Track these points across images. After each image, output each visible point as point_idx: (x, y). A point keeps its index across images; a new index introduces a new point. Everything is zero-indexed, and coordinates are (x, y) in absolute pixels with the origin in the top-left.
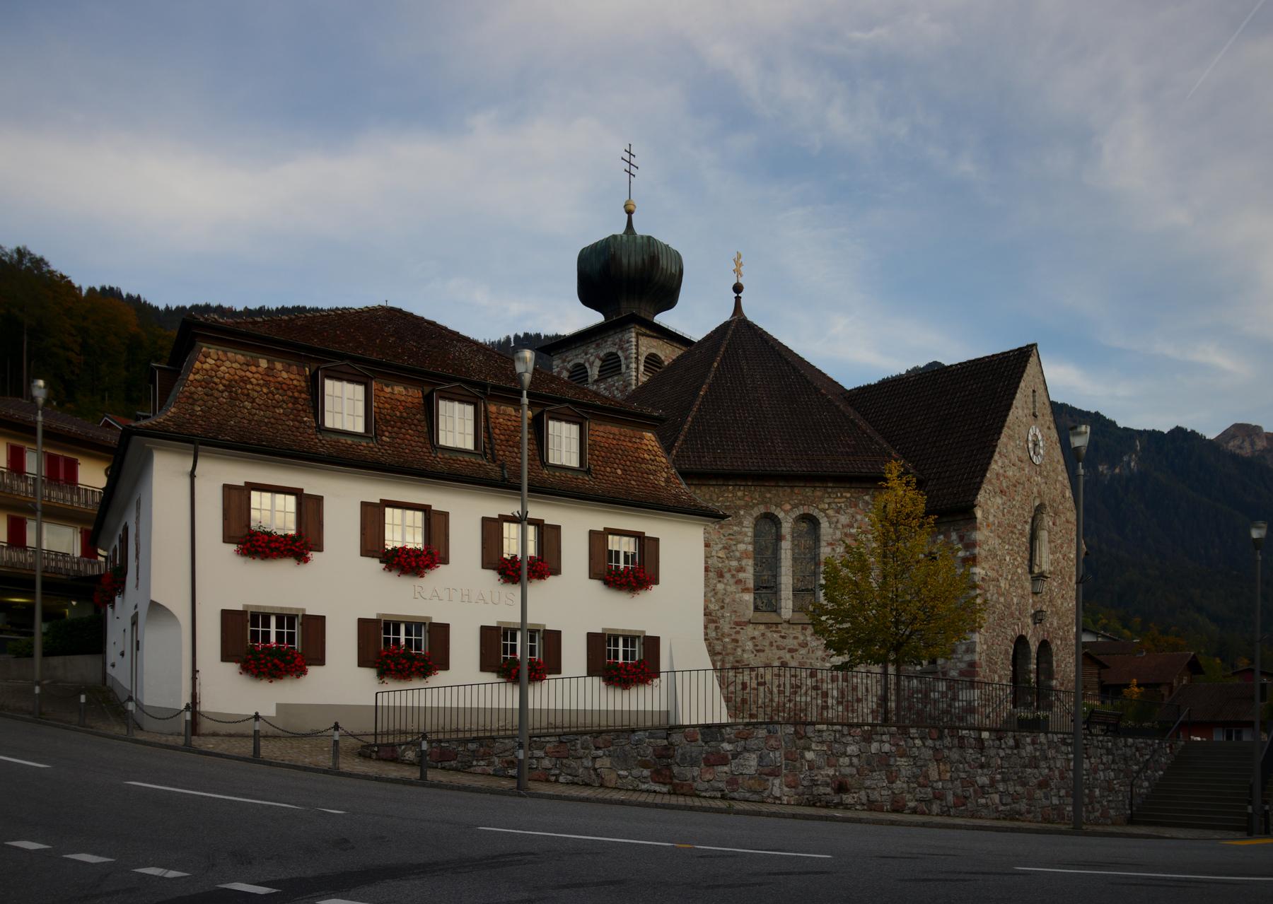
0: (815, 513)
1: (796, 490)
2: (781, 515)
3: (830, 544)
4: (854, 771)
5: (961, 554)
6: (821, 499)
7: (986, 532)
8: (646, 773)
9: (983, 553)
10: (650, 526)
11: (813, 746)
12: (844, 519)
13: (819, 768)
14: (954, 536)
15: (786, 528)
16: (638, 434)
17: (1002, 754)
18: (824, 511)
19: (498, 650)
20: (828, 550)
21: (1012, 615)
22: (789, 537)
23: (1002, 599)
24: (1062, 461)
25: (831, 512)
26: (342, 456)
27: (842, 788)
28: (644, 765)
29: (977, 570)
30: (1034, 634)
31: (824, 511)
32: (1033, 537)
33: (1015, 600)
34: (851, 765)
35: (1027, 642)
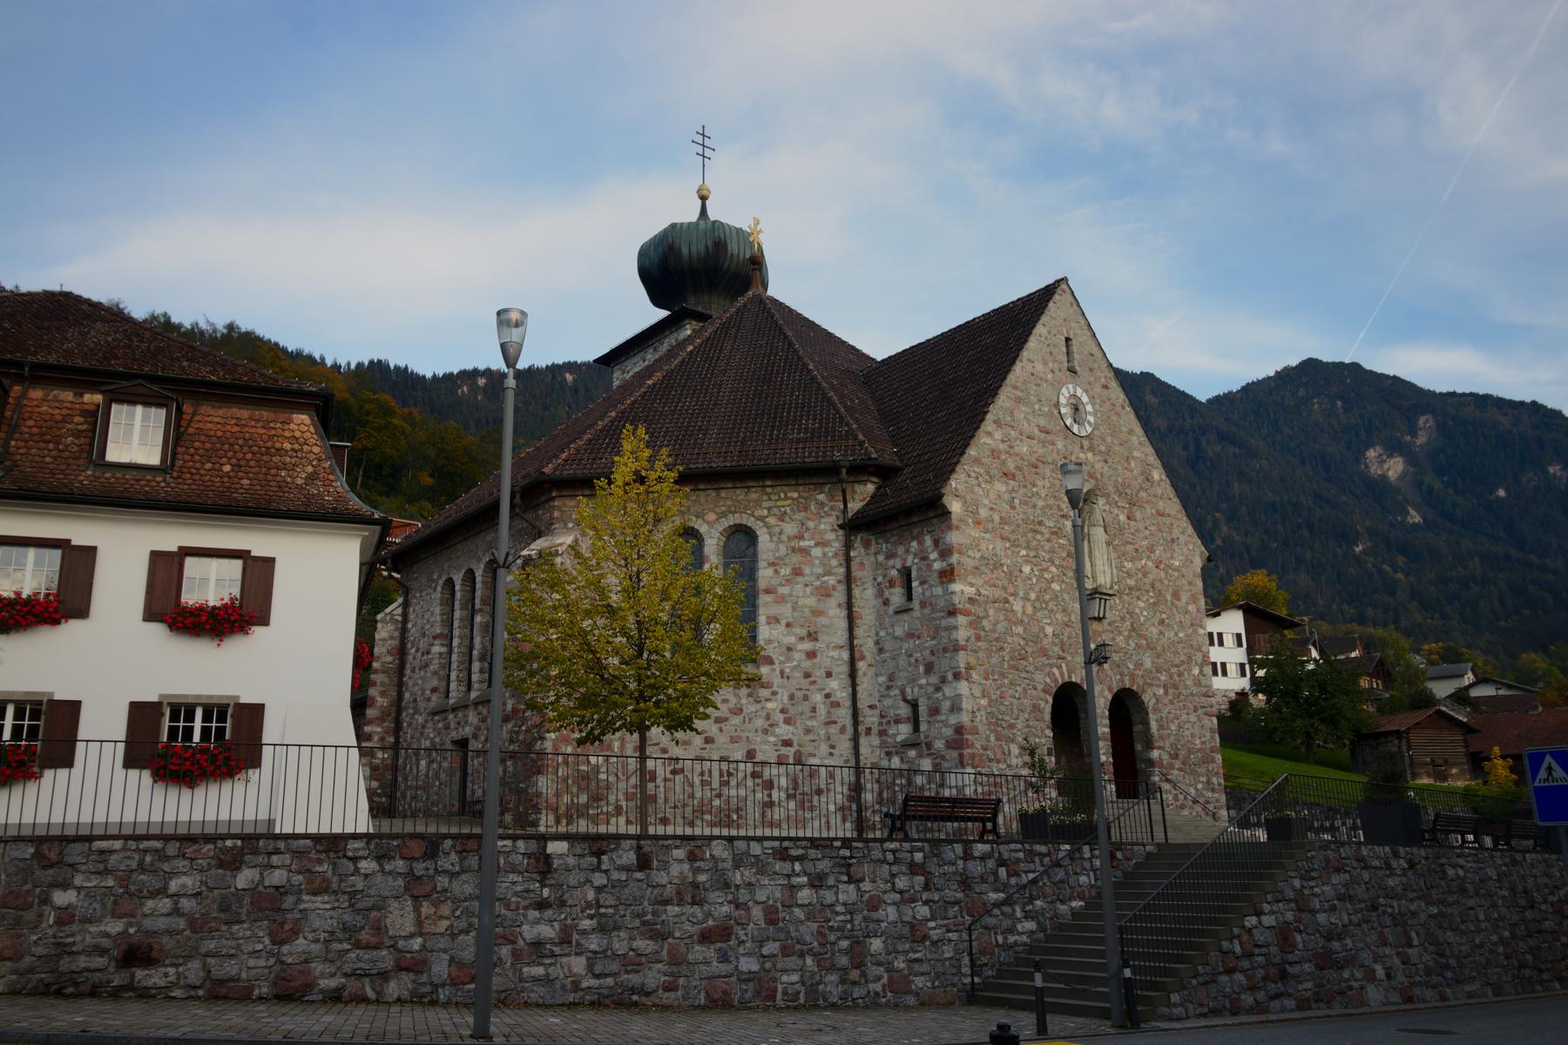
0: (751, 522)
1: (723, 494)
2: (703, 528)
4: (182, 923)
5: (937, 566)
6: (758, 503)
7: (975, 533)
9: (969, 563)
10: (259, 541)
11: (78, 880)
12: (790, 528)
13: (87, 920)
14: (928, 541)
16: (282, 417)
18: (762, 519)
20: (769, 572)
21: (1044, 652)
23: (1020, 630)
25: (772, 520)
26: (128, 495)
29: (956, 587)
31: (762, 519)
33: (1049, 630)
34: (176, 911)
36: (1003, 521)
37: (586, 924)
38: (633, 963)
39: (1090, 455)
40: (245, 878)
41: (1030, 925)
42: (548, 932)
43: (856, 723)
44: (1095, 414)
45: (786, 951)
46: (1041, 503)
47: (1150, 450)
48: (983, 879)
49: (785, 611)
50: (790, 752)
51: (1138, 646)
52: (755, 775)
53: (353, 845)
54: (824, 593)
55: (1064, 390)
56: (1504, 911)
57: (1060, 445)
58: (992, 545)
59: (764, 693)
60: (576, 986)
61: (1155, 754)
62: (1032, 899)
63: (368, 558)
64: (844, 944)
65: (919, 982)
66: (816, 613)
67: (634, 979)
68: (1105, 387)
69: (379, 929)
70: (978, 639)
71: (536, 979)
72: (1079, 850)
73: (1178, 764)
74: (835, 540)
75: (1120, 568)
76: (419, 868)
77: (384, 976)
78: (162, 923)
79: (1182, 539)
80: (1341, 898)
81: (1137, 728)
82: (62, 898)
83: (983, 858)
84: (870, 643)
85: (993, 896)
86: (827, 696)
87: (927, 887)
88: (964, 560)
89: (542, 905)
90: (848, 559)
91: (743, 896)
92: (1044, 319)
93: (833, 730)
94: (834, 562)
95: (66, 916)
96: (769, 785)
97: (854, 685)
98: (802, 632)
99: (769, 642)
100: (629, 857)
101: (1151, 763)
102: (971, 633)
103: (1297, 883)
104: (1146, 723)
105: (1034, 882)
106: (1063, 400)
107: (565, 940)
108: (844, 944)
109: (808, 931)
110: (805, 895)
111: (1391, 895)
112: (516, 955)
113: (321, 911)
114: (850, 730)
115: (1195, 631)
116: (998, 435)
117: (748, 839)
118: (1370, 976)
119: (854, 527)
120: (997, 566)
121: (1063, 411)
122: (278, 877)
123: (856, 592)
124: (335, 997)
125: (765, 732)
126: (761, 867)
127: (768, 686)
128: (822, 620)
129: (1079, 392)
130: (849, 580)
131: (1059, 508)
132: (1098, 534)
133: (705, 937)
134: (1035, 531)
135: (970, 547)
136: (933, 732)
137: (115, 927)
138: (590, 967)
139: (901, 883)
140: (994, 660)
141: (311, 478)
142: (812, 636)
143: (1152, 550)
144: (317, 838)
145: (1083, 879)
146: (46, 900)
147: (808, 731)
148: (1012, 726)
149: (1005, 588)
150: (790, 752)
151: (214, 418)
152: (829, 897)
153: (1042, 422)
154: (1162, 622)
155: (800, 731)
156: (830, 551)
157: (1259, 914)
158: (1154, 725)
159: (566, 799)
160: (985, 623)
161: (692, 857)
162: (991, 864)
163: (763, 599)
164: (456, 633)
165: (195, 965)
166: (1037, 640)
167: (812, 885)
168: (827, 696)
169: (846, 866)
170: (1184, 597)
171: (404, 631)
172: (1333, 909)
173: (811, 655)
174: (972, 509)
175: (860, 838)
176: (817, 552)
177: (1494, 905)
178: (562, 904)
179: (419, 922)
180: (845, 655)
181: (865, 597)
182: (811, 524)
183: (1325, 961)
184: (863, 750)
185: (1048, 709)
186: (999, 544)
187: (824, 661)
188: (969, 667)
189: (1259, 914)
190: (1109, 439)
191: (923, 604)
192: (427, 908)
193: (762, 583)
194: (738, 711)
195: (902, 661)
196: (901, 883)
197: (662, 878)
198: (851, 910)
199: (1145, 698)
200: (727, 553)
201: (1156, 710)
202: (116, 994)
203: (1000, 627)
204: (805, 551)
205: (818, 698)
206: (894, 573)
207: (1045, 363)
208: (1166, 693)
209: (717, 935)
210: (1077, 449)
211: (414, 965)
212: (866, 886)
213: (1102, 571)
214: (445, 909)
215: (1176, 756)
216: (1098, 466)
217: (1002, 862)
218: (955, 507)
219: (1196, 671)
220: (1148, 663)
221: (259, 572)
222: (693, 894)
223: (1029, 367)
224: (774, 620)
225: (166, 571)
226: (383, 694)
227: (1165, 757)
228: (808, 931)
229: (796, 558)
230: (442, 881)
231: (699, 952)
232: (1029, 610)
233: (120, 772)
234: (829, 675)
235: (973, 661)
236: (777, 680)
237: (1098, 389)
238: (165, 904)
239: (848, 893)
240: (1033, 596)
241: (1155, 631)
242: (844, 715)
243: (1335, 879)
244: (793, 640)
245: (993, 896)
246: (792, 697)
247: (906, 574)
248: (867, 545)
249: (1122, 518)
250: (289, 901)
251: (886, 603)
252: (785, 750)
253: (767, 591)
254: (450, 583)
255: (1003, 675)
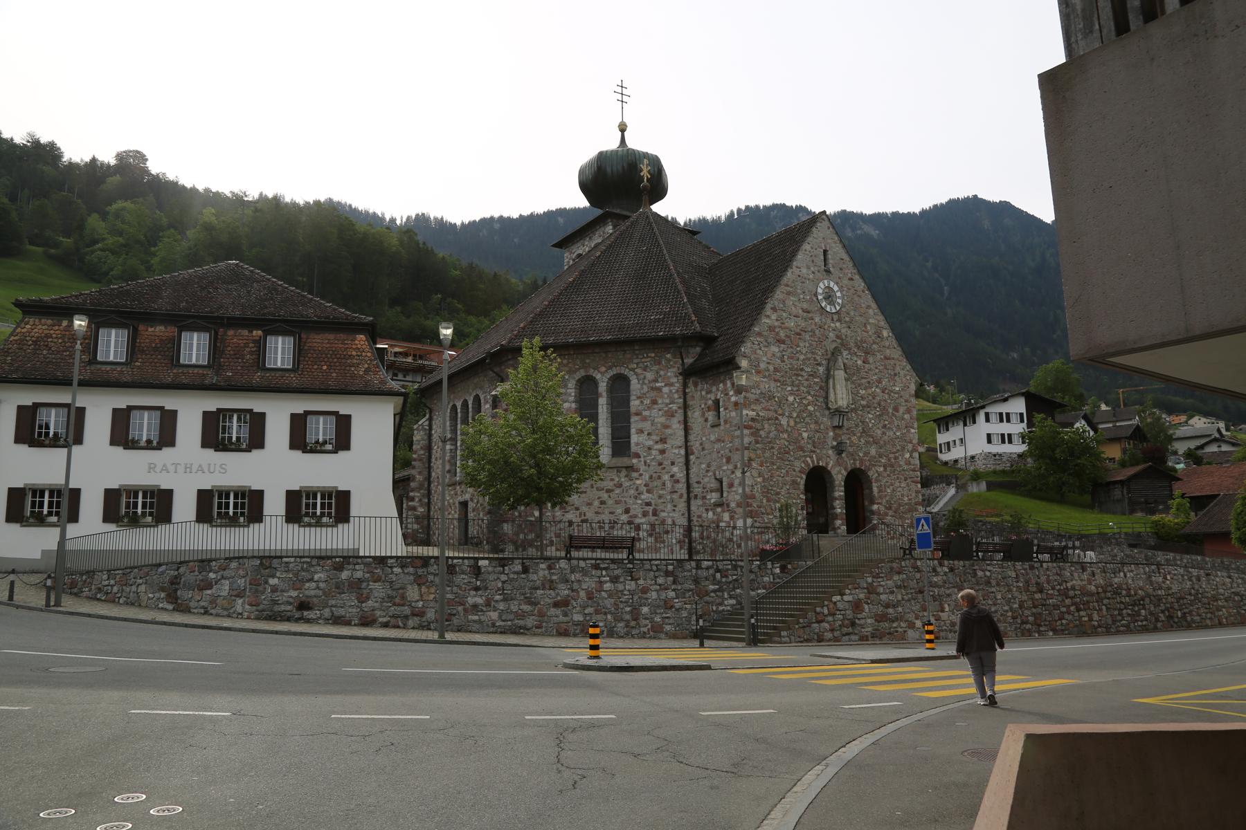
0: (626, 372)
2: (598, 377)
3: (639, 398)
5: (733, 399)
8: (163, 595)
10: (343, 406)
11: (278, 574)
12: (650, 376)
13: (283, 591)
15: (603, 387)
17: (504, 578)
19: (211, 506)
20: (637, 402)
21: (801, 449)
22: (604, 394)
23: (786, 436)
24: (874, 305)
27: (303, 606)
28: (162, 589)
30: (838, 463)
31: (633, 370)
32: (828, 376)
33: (805, 435)
35: (829, 472)
36: (776, 370)
37: (498, 597)
38: (521, 615)
39: (838, 324)
40: (345, 575)
41: (733, 602)
42: (479, 601)
43: (689, 492)
44: (843, 298)
45: (597, 612)
46: (802, 357)
47: (881, 317)
48: (706, 579)
49: (647, 426)
50: (650, 509)
51: (867, 442)
52: (630, 523)
53: (390, 561)
54: (671, 414)
55: (821, 285)
56: (1016, 594)
57: (817, 320)
58: (767, 385)
59: (635, 475)
60: (494, 625)
61: (875, 507)
62: (734, 589)
63: (399, 410)
64: (628, 609)
65: (668, 628)
66: (667, 427)
67: (521, 623)
68: (851, 279)
69: (403, 597)
70: (757, 442)
71: (475, 621)
72: (765, 564)
73: (891, 513)
74: (677, 382)
75: (855, 394)
76: (420, 571)
77: (406, 617)
78: (312, 593)
79: (902, 373)
80: (899, 587)
81: (866, 492)
82: (273, 581)
83: (708, 568)
84: (697, 444)
85: (712, 587)
86: (672, 476)
87: (674, 582)
88: (748, 395)
89: (477, 589)
90: (685, 394)
91: (575, 586)
92: (810, 239)
93: (675, 496)
94: (676, 396)
95: (275, 589)
96: (638, 528)
97: (688, 470)
98: (658, 438)
99: (637, 444)
100: (519, 568)
101: (873, 513)
102: (752, 439)
103: (870, 580)
104: (871, 489)
105: (736, 580)
106: (820, 291)
107: (488, 604)
108: (628, 609)
109: (609, 603)
110: (607, 586)
111: (935, 585)
112: (465, 610)
113: (378, 589)
114: (685, 496)
115: (909, 431)
116: (774, 317)
117: (579, 559)
118: (911, 626)
119: (688, 374)
120: (771, 398)
121: (820, 297)
122: (359, 574)
123: (689, 414)
124: (385, 625)
125: (636, 498)
126: (584, 572)
127: (637, 470)
128: (669, 431)
129: (832, 284)
130: (685, 407)
131: (815, 359)
132: (840, 375)
133: (556, 605)
134: (798, 375)
135: (752, 387)
136: (730, 498)
137: (294, 594)
138: (500, 617)
139: (660, 580)
140: (767, 455)
141: (367, 371)
142: (663, 441)
143: (879, 381)
144: (375, 558)
145: (766, 579)
146: (266, 582)
147: (660, 497)
148: (778, 494)
149: (776, 411)
150: (650, 509)
151: (318, 341)
152: (620, 587)
153: (805, 306)
154: (885, 426)
155: (656, 496)
156: (674, 389)
157: (842, 594)
158: (875, 490)
159: (522, 536)
160: (762, 433)
161: (550, 568)
162: (711, 571)
163: (634, 419)
164: (459, 437)
165: (327, 610)
166: (797, 441)
167: (611, 581)
168: (672, 476)
169: (630, 572)
170: (902, 410)
171: (430, 435)
172: (892, 592)
173: (662, 452)
174: (755, 365)
175: (690, 559)
176: (666, 390)
177: (1010, 591)
178: (486, 588)
179: (421, 596)
180: (683, 452)
181: (695, 416)
182: (662, 373)
183: (880, 618)
184: (693, 508)
185: (803, 482)
186: (773, 384)
187: (670, 455)
188: (750, 460)
189: (842, 594)
190: (852, 313)
191: (726, 422)
192: (424, 589)
193: (633, 410)
194: (620, 485)
195: (714, 455)
196: (660, 580)
197: (534, 577)
198: (632, 593)
199: (870, 473)
200: (611, 390)
201: (877, 481)
202: (297, 620)
203: (771, 435)
204: (659, 389)
205: (666, 477)
206: (710, 402)
207: (808, 268)
208: (885, 470)
209: (562, 604)
210: (829, 321)
211: (420, 614)
212: (641, 582)
213: (841, 396)
214: (432, 590)
215: (890, 508)
216: (843, 331)
217: (718, 570)
218: (744, 363)
219: (907, 455)
220: (873, 452)
221: (343, 424)
222: (551, 585)
223: (797, 272)
224: (640, 431)
225: (298, 424)
226: (420, 473)
227: (882, 509)
228: (609, 603)
229: (653, 394)
230: (431, 578)
231: (553, 611)
232: (792, 423)
233: (285, 525)
234: (673, 464)
235: (753, 456)
236: (642, 468)
237: (845, 281)
238: (313, 585)
239: (631, 585)
240: (795, 415)
241: (879, 432)
242: (682, 487)
243: (896, 577)
244: (651, 443)
245: (712, 587)
246: (651, 477)
247: (717, 402)
248: (696, 385)
249: (859, 362)
250: (364, 584)
251: (706, 420)
252: (647, 508)
253: (637, 414)
254: (454, 407)
255: (773, 464)
